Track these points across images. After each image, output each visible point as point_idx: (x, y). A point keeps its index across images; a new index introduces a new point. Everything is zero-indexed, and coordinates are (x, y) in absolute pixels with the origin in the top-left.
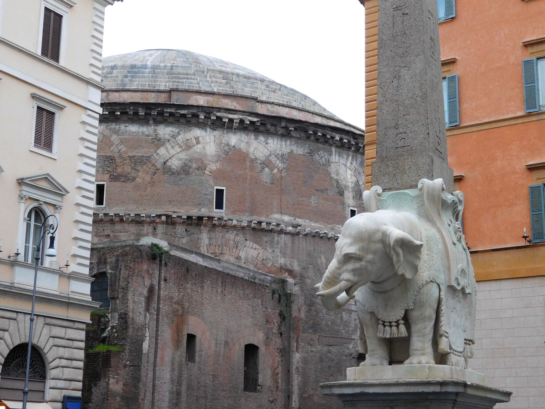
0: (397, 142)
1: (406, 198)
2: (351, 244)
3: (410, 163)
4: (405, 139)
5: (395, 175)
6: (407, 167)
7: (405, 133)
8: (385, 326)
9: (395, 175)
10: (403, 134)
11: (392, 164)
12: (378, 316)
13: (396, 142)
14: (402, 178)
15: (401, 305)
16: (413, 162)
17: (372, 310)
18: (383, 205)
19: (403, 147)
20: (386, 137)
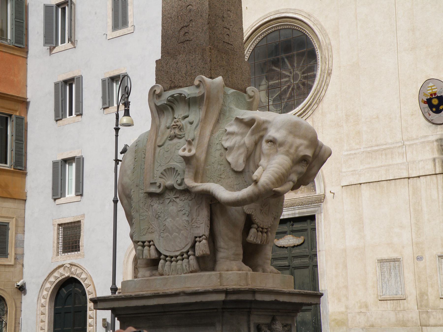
0: (225, 36)
1: (242, 101)
2: (308, 147)
3: (237, 64)
4: (229, 35)
5: (227, 72)
6: (235, 68)
7: (229, 29)
8: (258, 231)
9: (227, 72)
10: (227, 30)
11: (225, 59)
12: (255, 219)
13: (223, 35)
14: (232, 77)
15: (274, 213)
16: (239, 64)
17: (251, 213)
18: (225, 100)
19: (228, 43)
20: (216, 25)
